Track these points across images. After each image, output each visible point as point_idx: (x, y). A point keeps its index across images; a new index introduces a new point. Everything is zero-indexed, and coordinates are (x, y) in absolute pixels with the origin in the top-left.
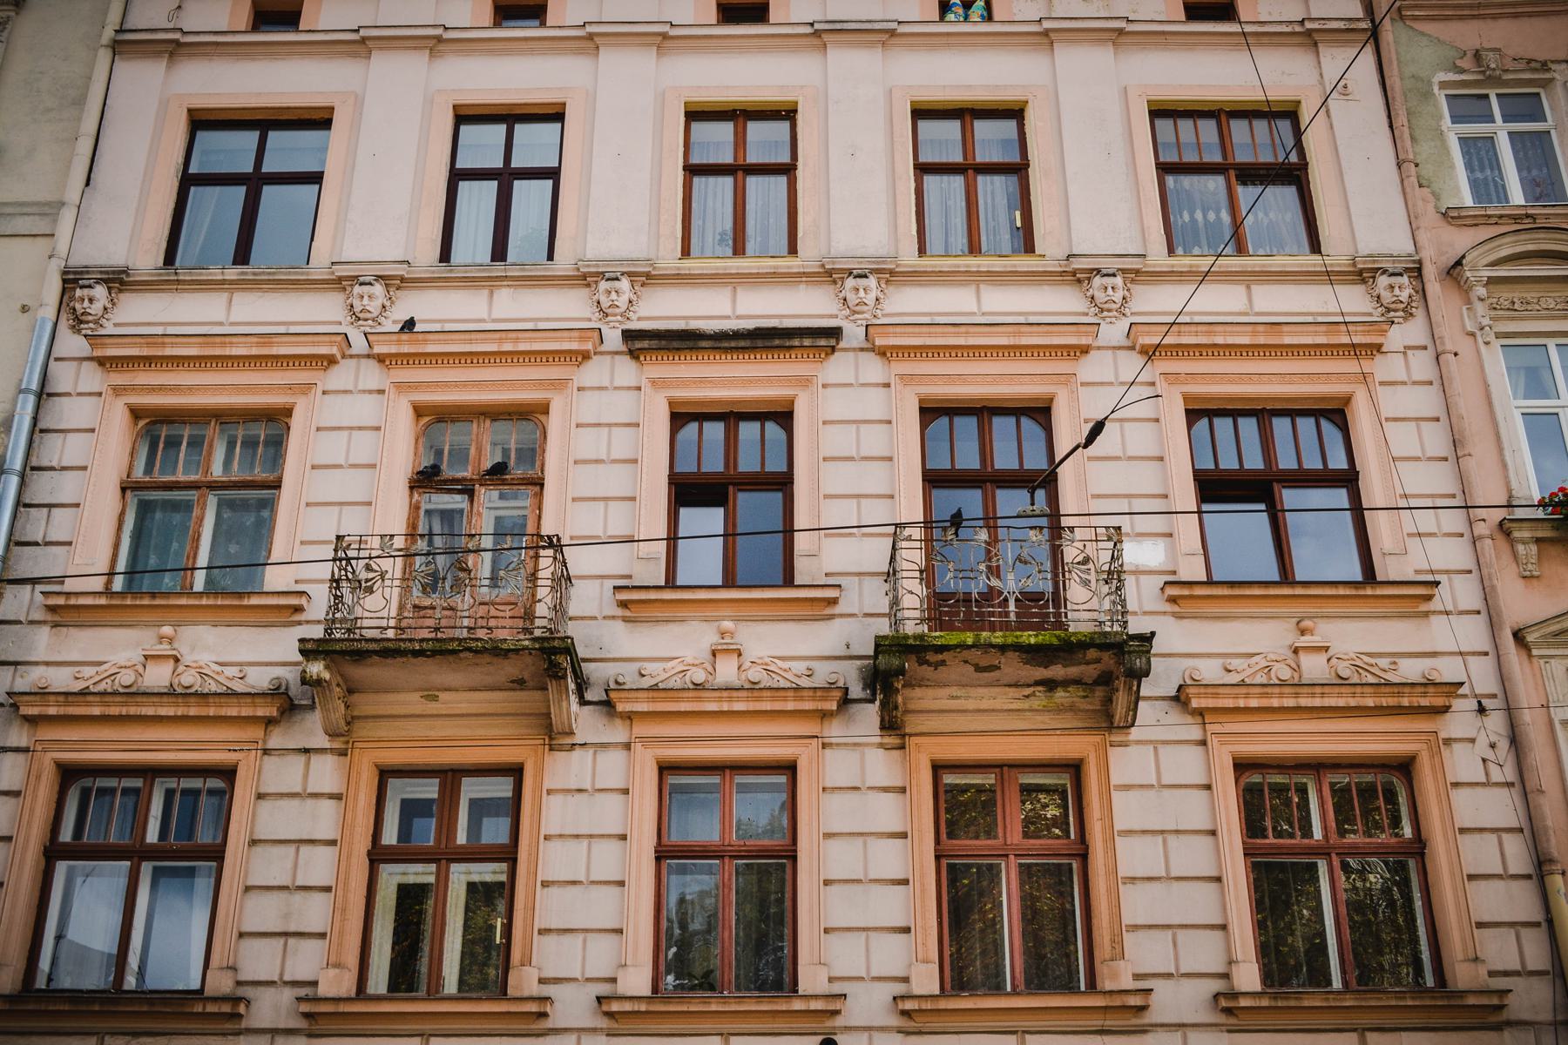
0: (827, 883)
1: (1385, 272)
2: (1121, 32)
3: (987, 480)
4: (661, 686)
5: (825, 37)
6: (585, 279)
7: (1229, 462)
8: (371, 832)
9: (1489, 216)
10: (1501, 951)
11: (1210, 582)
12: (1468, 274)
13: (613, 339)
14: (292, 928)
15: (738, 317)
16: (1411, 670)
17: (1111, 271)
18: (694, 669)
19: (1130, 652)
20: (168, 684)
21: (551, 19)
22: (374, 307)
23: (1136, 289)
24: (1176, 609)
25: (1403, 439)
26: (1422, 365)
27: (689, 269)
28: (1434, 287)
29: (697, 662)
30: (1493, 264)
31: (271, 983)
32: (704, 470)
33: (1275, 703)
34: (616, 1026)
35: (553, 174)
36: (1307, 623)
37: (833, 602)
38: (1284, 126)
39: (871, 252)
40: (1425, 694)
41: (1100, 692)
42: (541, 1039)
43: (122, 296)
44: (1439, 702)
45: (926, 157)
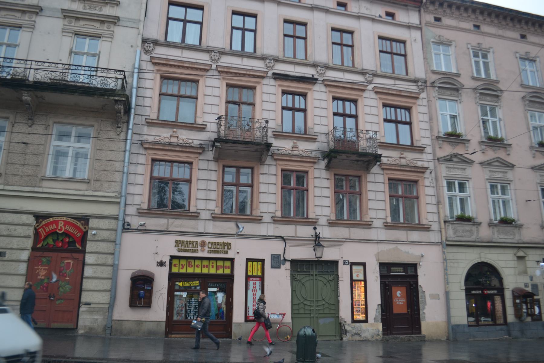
0: (315, 196)
3: (344, 115)
7: (389, 118)
9: (439, 73)
10: (431, 217)
13: (270, 74)
14: (208, 198)
16: (419, 164)
22: (217, 58)
25: (421, 117)
26: (425, 102)
30: (440, 83)
33: (397, 168)
35: (255, 31)
38: (402, 45)
40: (422, 169)
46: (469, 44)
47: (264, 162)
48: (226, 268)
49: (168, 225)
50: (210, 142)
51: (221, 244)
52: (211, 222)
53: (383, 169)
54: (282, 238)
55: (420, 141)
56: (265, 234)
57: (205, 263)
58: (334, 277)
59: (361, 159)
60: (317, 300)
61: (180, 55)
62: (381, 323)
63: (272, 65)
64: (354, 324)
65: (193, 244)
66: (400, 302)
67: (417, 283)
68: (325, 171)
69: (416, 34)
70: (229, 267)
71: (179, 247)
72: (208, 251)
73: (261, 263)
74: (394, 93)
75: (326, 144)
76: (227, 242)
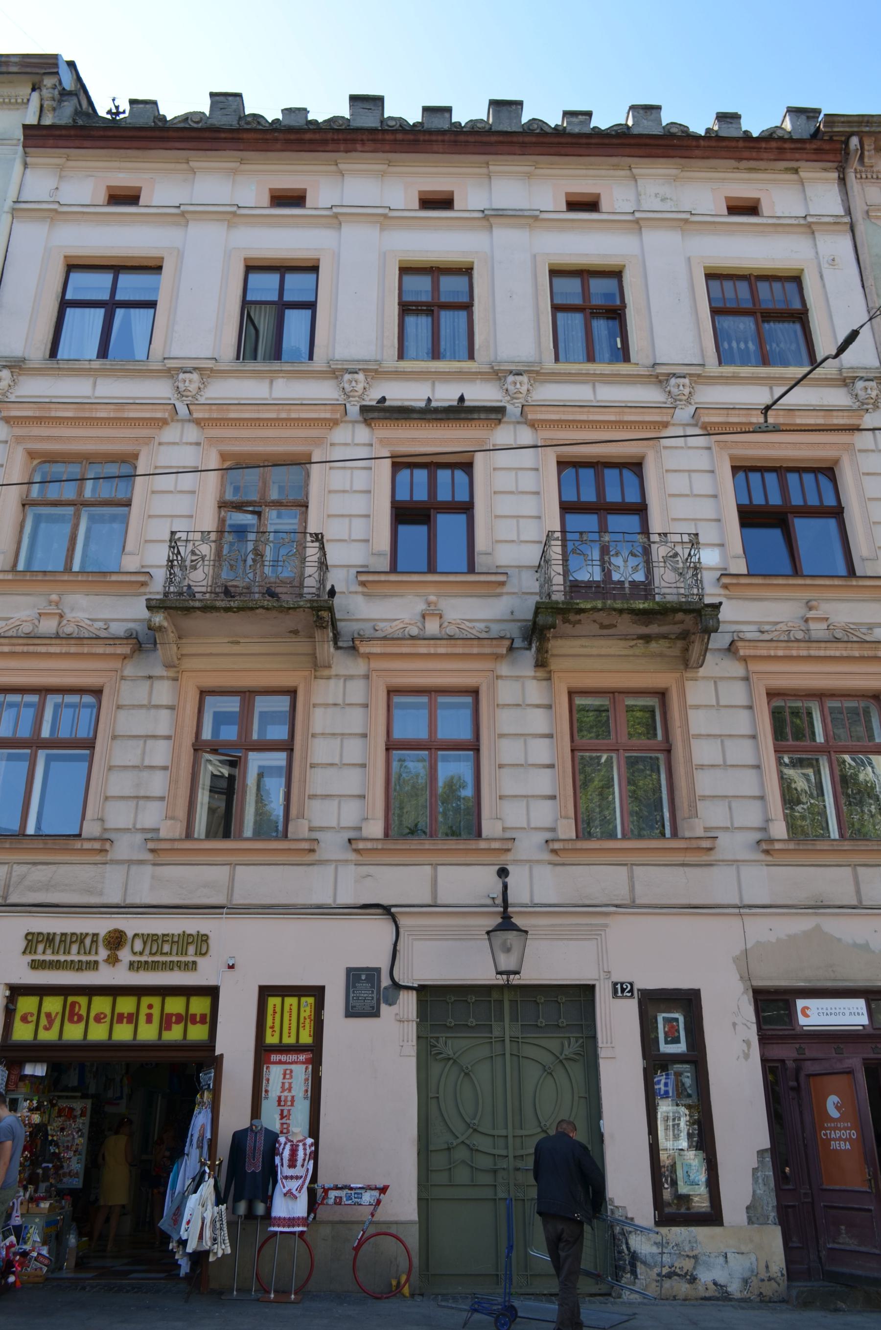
2: (686, 221)
5: (492, 220)
6: (334, 373)
8: (194, 731)
11: (749, 575)
13: (354, 410)
14: (142, 794)
17: (682, 375)
18: (410, 627)
19: (705, 615)
20: (54, 631)
21: (309, 202)
23: (699, 388)
24: (727, 592)
27: (404, 368)
29: (412, 622)
31: (127, 830)
32: (415, 499)
33: (794, 653)
34: (361, 858)
35: (311, 306)
36: (814, 603)
37: (503, 584)
38: (791, 287)
39: (524, 359)
41: (680, 644)
42: (311, 867)
43: (20, 378)
45: (558, 301)
48: (194, 1022)
49: (7, 886)
51: (176, 939)
52: (148, 870)
54: (386, 910)
56: (329, 901)
57: (126, 1005)
58: (582, 1046)
60: (519, 1132)
62: (779, 1228)
64: (664, 1230)
65: (82, 942)
66: (840, 1139)
68: (535, 682)
72: (131, 964)
73: (311, 1000)
76: (194, 932)
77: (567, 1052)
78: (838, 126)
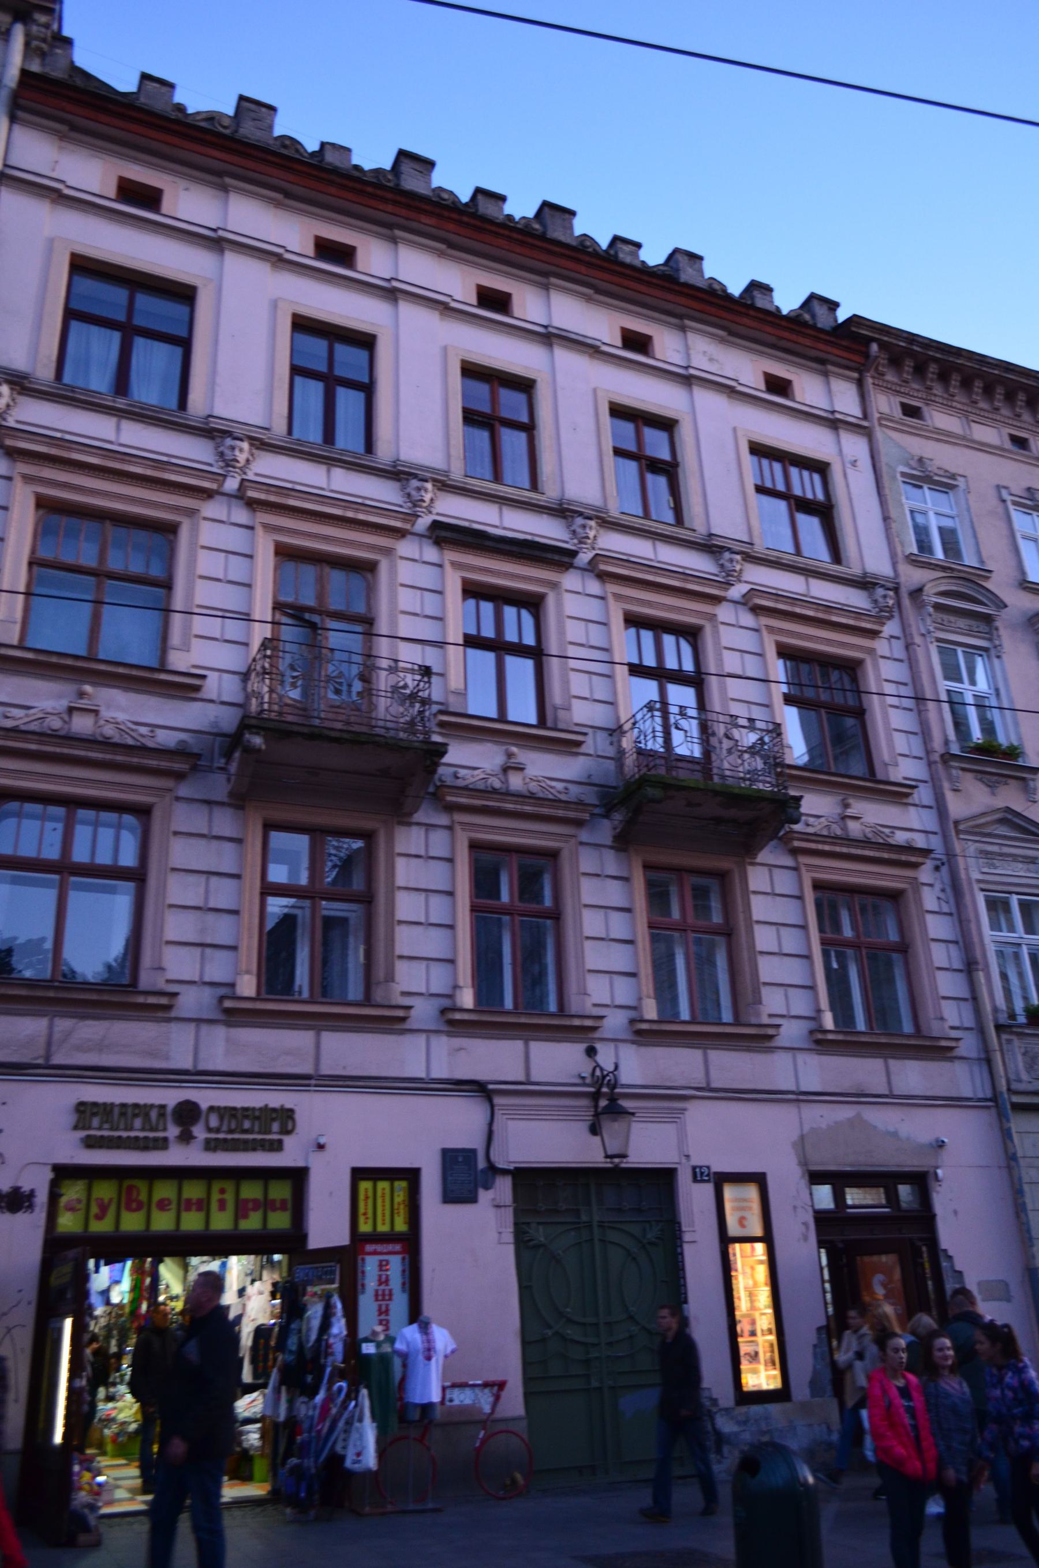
1: (882, 586)
4: (471, 786)
9: (931, 564)
12: (925, 598)
13: (423, 523)
14: (209, 941)
15: (505, 528)
16: (900, 838)
26: (898, 649)
28: (906, 602)
33: (838, 849)
44: (920, 860)
46: (1006, 488)
47: (411, 814)
48: (274, 1209)
49: (49, 1044)
50: (219, 739)
51: (257, 1113)
52: (220, 1032)
53: (795, 852)
55: (896, 765)
56: (423, 1075)
57: (193, 1190)
59: (733, 813)
61: (111, 436)
63: (427, 497)
64: (743, 1409)
65: (147, 1115)
67: (932, 1241)
68: (612, 852)
69: (855, 446)
70: (284, 1202)
71: (90, 1128)
73: (404, 1184)
74: (810, 613)
75: (611, 765)
77: (650, 1236)
78: (863, 329)
